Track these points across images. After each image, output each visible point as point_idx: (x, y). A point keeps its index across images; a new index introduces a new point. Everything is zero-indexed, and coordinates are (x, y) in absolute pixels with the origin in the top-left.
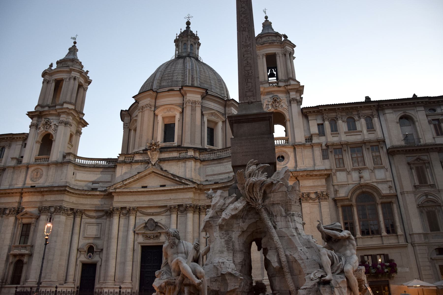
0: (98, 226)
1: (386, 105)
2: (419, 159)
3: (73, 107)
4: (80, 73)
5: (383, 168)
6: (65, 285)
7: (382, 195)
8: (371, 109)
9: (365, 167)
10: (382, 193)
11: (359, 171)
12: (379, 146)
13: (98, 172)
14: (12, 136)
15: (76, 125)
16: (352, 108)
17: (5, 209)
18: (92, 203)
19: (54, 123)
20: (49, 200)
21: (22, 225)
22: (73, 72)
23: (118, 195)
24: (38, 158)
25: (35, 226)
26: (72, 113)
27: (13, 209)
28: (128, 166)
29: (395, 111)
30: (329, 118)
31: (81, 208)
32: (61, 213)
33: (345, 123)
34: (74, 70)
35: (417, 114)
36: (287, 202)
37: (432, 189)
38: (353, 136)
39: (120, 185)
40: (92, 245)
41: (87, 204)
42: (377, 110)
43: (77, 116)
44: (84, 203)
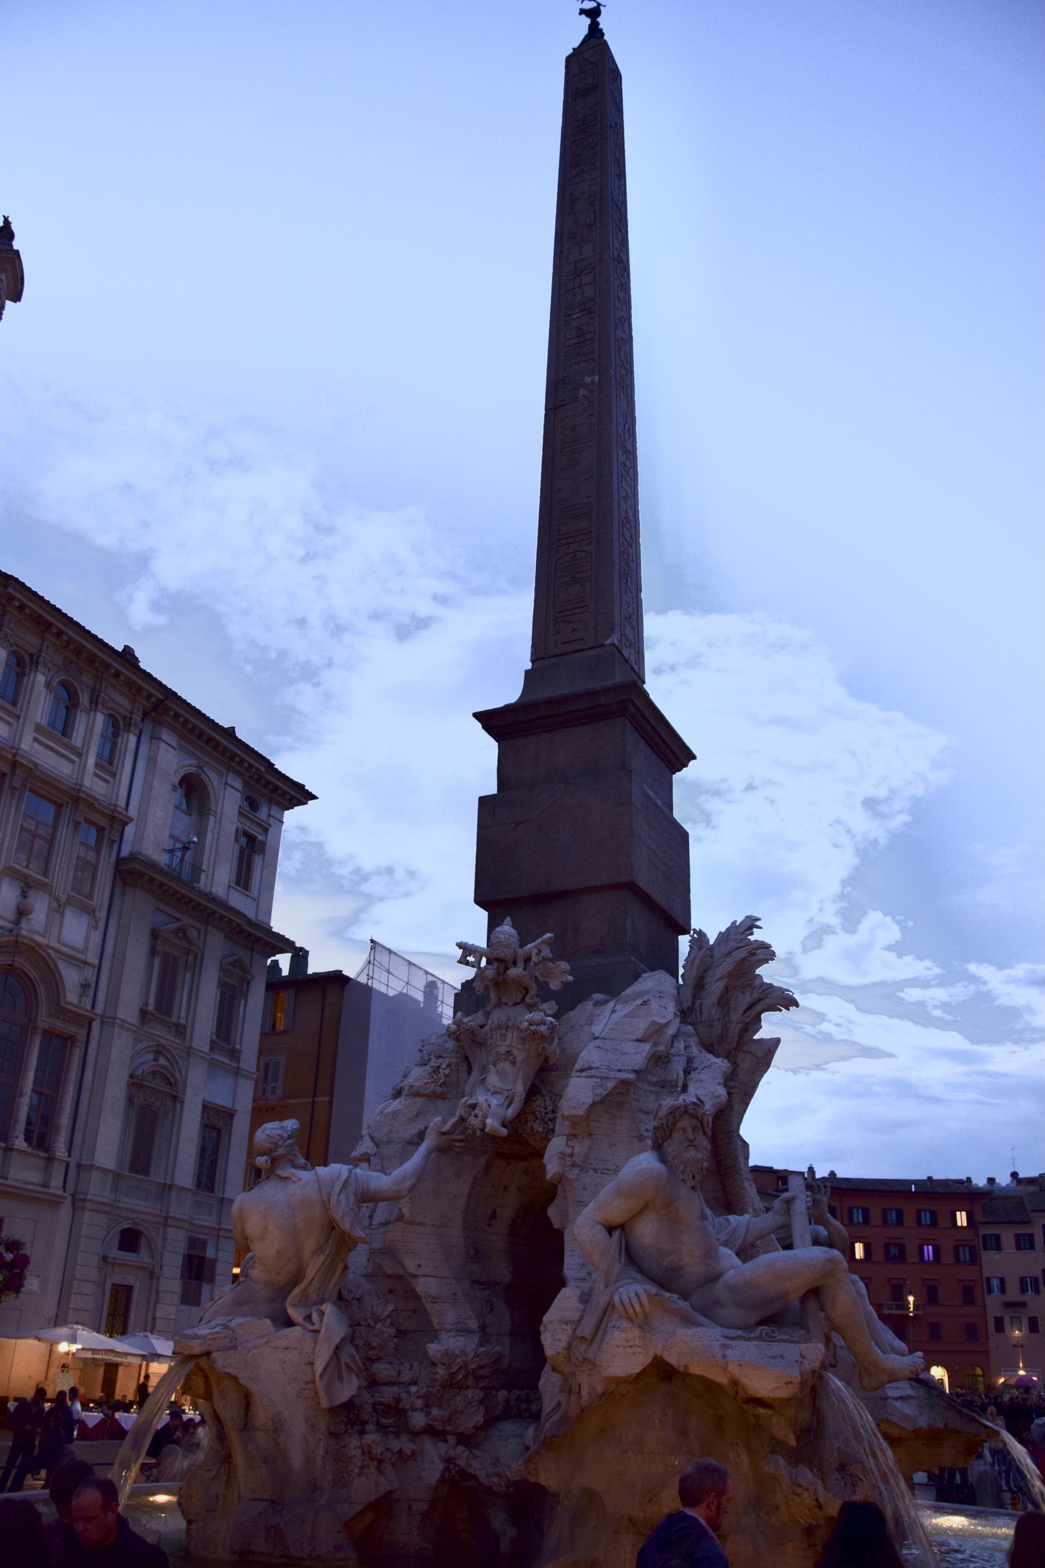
1: (177, 716)
2: (181, 932)
5: (89, 913)
7: (63, 1004)
8: (134, 701)
9: (43, 879)
10: (65, 997)
11: (22, 884)
12: (107, 832)
16: (92, 659)
29: (181, 748)
30: (17, 645)
33: (51, 692)
35: (222, 792)
36: (746, 1094)
37: (177, 1041)
38: (50, 754)
42: (145, 715)
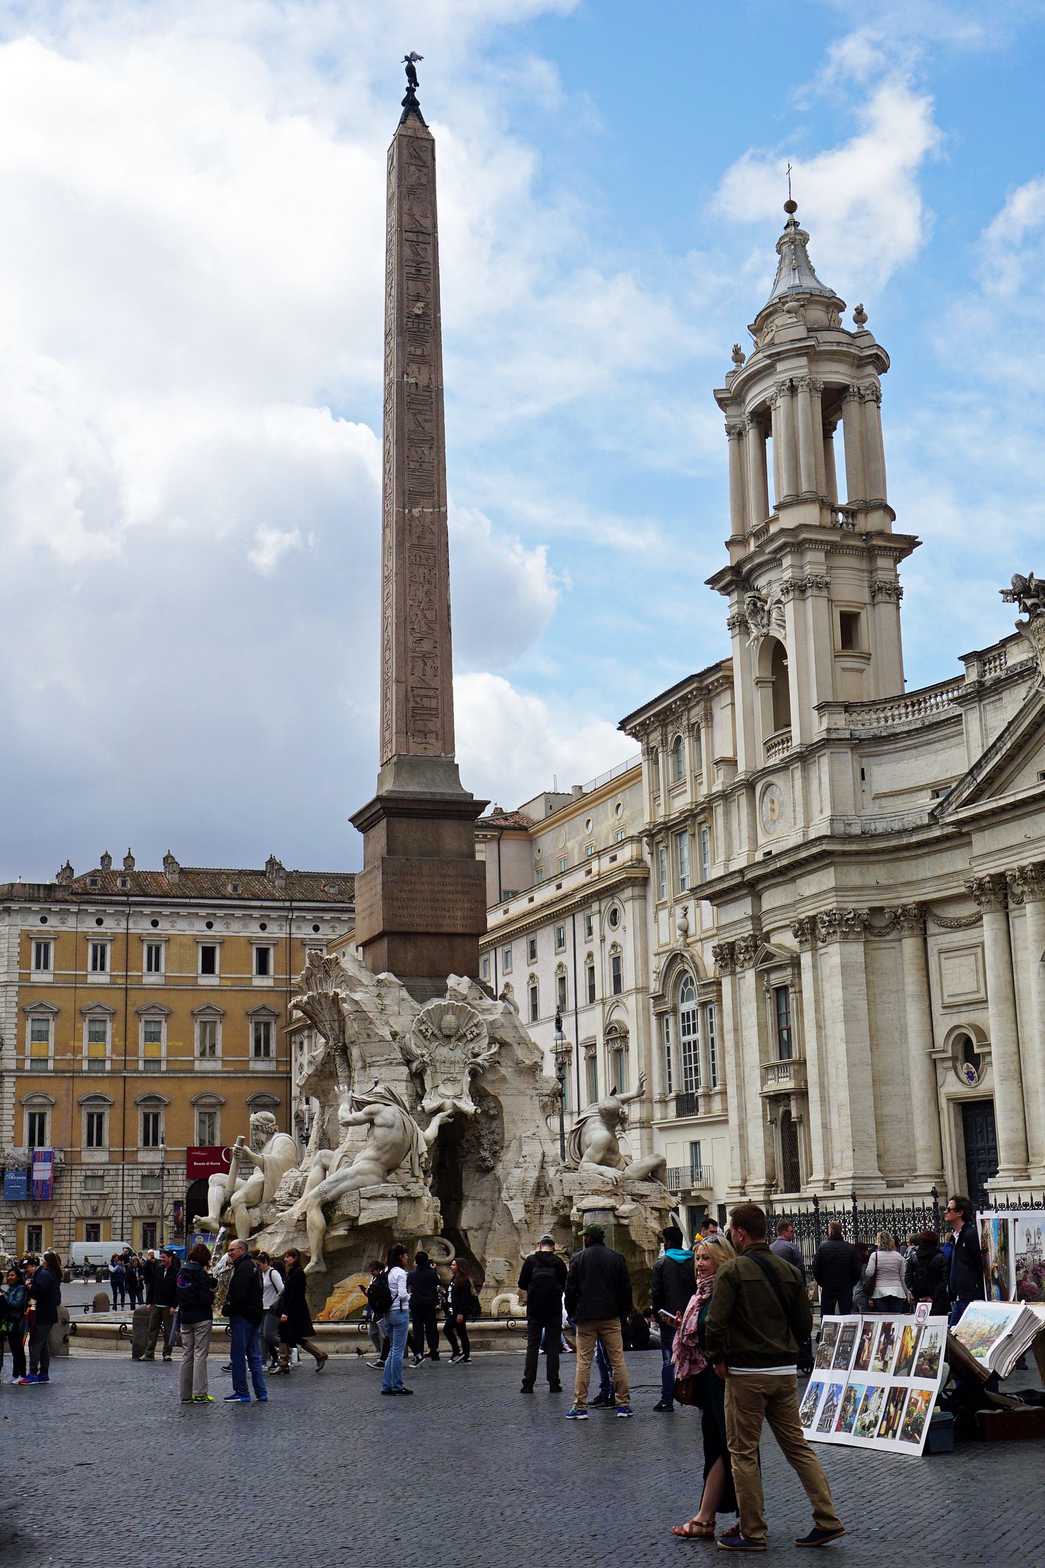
0: (973, 958)
3: (810, 515)
4: (806, 354)
6: (909, 1188)
13: (939, 741)
14: (701, 682)
15: (865, 566)
17: (732, 946)
18: (939, 872)
19: (775, 600)
20: (807, 894)
21: (772, 993)
22: (780, 367)
23: (981, 829)
24: (779, 739)
25: (801, 992)
26: (810, 541)
27: (743, 944)
28: (993, 699)
31: (911, 897)
32: (839, 934)
34: (778, 354)
39: (969, 788)
40: (964, 1031)
41: (924, 880)
43: (838, 539)
44: (914, 878)
